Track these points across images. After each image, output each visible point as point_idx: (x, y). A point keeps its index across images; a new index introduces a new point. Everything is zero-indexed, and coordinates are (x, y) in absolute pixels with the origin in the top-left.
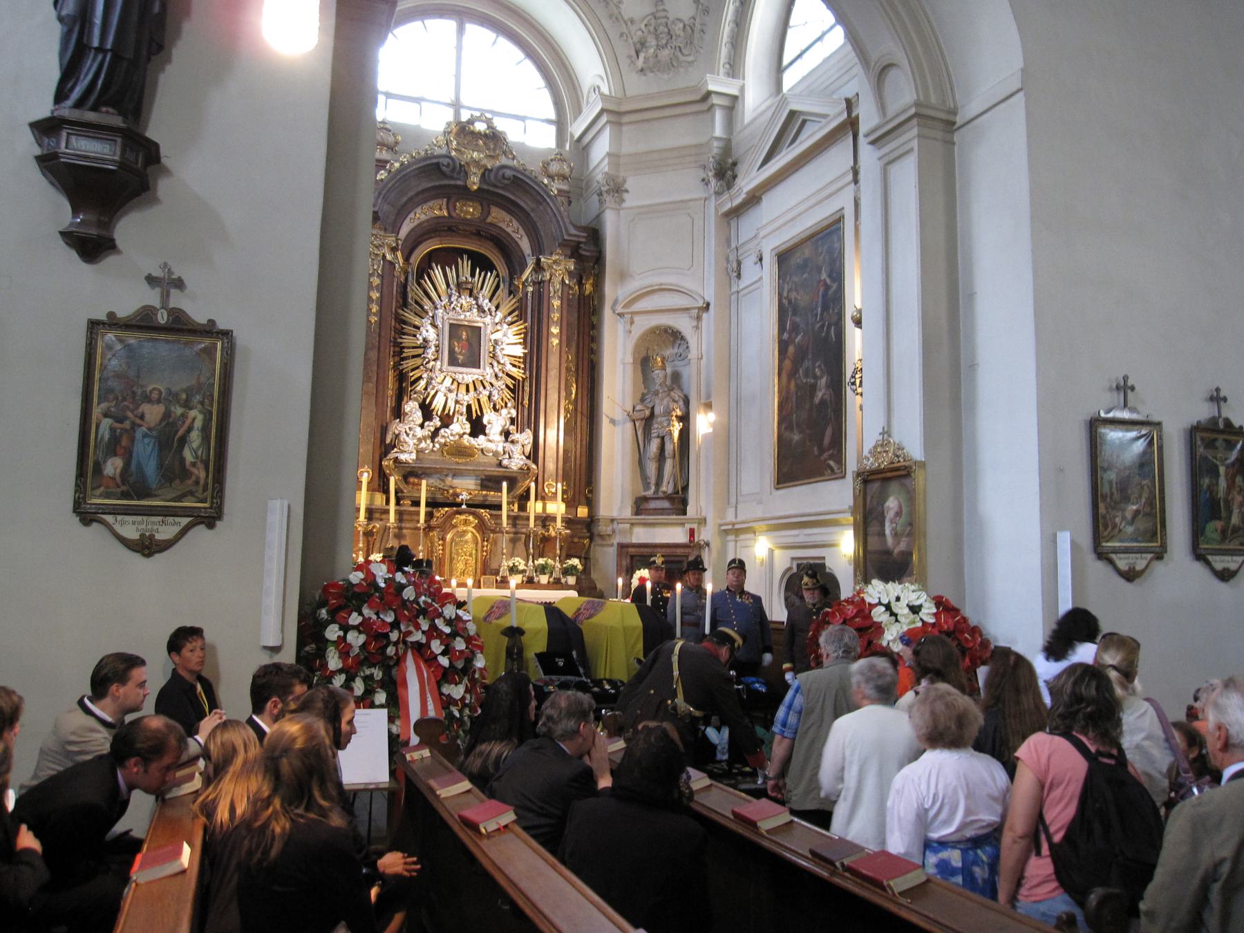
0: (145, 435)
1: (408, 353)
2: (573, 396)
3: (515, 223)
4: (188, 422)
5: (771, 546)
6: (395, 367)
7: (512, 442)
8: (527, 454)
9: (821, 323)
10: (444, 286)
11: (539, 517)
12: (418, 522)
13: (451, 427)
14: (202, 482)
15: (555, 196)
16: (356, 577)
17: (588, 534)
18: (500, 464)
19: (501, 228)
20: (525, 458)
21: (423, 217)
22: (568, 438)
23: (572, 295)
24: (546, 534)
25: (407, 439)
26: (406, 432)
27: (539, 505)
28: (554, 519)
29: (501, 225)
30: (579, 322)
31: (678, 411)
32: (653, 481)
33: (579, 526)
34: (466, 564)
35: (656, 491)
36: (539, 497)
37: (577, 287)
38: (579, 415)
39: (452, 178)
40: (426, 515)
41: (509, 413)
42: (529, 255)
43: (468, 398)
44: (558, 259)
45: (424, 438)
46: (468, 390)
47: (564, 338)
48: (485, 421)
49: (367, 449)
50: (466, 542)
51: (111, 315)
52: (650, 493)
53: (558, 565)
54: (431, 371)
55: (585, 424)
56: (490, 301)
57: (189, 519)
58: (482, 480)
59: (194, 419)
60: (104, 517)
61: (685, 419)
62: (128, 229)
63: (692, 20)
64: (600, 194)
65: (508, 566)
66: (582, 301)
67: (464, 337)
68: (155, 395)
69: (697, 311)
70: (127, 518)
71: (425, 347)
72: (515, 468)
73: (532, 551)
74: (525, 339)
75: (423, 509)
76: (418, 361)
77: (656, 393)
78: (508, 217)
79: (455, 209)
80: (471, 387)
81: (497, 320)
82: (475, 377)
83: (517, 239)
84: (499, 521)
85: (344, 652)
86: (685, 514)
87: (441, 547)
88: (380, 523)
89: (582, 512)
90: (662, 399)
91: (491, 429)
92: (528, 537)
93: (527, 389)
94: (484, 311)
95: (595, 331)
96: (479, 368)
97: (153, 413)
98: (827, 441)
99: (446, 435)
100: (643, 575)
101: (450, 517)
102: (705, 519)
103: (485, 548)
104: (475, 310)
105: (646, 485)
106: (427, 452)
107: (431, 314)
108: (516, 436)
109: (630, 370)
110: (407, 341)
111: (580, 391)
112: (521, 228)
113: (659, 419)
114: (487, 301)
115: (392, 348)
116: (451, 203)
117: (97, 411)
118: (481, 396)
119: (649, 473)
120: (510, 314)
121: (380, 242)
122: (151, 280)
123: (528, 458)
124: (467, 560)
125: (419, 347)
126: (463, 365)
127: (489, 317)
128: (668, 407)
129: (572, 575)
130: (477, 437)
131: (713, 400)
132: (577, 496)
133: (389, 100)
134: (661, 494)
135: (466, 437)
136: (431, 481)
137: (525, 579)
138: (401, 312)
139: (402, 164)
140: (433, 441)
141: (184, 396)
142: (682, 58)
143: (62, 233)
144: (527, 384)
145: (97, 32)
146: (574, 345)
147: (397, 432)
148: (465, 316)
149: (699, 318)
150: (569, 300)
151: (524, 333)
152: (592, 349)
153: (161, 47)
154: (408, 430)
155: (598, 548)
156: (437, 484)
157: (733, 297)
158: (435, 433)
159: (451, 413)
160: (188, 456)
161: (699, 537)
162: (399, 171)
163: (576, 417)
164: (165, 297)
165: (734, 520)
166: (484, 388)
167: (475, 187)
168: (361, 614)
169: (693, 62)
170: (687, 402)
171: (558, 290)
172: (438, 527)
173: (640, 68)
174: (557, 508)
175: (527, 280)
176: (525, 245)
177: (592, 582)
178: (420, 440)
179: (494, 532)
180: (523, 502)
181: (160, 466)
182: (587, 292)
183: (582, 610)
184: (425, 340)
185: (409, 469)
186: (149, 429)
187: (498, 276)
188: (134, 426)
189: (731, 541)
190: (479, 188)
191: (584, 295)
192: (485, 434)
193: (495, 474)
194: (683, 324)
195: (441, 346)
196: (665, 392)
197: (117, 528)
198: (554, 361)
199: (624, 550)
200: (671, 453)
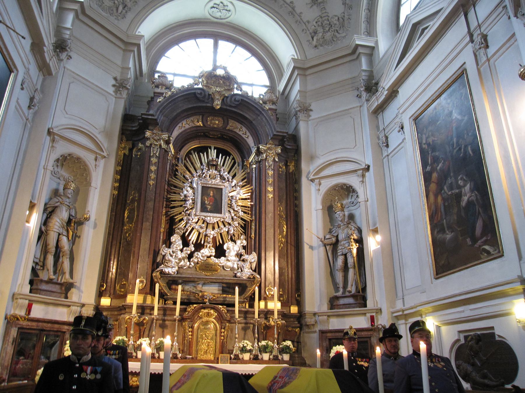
1: (174, 204)
2: (285, 233)
3: (244, 129)
5: (437, 323)
6: (166, 214)
7: (243, 261)
8: (253, 268)
9: (457, 149)
10: (199, 165)
11: (262, 311)
12: (175, 315)
13: (202, 251)
15: (267, 110)
17: (298, 325)
18: (235, 276)
19: (235, 132)
20: (251, 271)
21: (187, 126)
22: (282, 260)
23: (281, 171)
24: (268, 323)
25: (170, 258)
26: (170, 254)
27: (262, 304)
28: (271, 312)
29: (235, 130)
30: (286, 187)
31: (355, 235)
32: (341, 285)
33: (292, 319)
34: (208, 345)
35: (344, 292)
36: (262, 298)
37: (284, 167)
38: (289, 245)
39: (203, 102)
40: (180, 311)
41: (242, 243)
42: (253, 147)
43: (212, 233)
44: (271, 147)
45: (184, 259)
46: (213, 228)
47: (276, 193)
48: (225, 247)
50: (209, 329)
52: (340, 294)
53: (276, 345)
54: (189, 215)
55: (293, 251)
56: (229, 173)
58: (223, 287)
61: (360, 241)
63: (343, 14)
64: (296, 115)
65: (239, 347)
66: (288, 177)
67: (211, 194)
69: (362, 171)
71: (185, 201)
72: (245, 278)
73: (257, 336)
74: (251, 196)
75: (178, 306)
76: (180, 209)
77: (339, 226)
78: (239, 126)
79: (207, 122)
80: (216, 226)
81: (233, 184)
82: (219, 219)
83: (245, 138)
84: (233, 315)
86: (365, 306)
87: (190, 333)
88: (149, 316)
89: (294, 309)
90: (343, 230)
91: (229, 252)
92: (254, 326)
93: (253, 227)
94: (224, 179)
95: (297, 194)
96: (221, 213)
98: (478, 230)
99: (198, 256)
100: (339, 350)
101: (197, 311)
102: (381, 310)
104: (219, 178)
105: (337, 289)
106: (185, 268)
107: (190, 181)
108: (246, 257)
109: (320, 213)
110: (173, 197)
111: (289, 230)
112: (247, 131)
113: (342, 243)
114: (226, 173)
115: (165, 203)
116: (204, 118)
118: (222, 231)
119: (338, 281)
120: (242, 180)
121: (158, 138)
123: (255, 271)
124: (209, 343)
125: (181, 201)
126: (211, 212)
127: (228, 182)
128: (348, 234)
129: (287, 353)
130: (220, 258)
131: (378, 225)
132: (290, 299)
133: (175, 77)
134: (347, 294)
135: (212, 258)
136: (187, 287)
137: (252, 356)
138: (170, 179)
140: (189, 261)
142: (338, 35)
144: (253, 224)
146: (284, 202)
147: (163, 254)
148: (212, 182)
149: (363, 176)
150: (279, 174)
151: (251, 192)
152: (296, 204)
154: (171, 253)
155: (305, 335)
156: (191, 289)
157: (385, 160)
158: (190, 256)
159: (202, 242)
161: (377, 322)
162: (170, 97)
163: (287, 246)
165: (403, 308)
166: (225, 226)
167: (218, 107)
169: (345, 36)
170: (360, 231)
171: (271, 165)
172: (189, 319)
173: (315, 45)
174: (275, 305)
175: (252, 161)
176: (250, 141)
177: (303, 359)
178: (180, 260)
179: (229, 322)
180: (251, 302)
182: (291, 171)
183: (277, 379)
184: (186, 196)
185: (171, 279)
187: (233, 159)
189: (402, 324)
190: (220, 108)
191: (289, 173)
192: (225, 256)
193: (230, 281)
194: (353, 181)
195: (196, 200)
196: (345, 225)
198: (270, 208)
199: (324, 335)
200: (352, 264)
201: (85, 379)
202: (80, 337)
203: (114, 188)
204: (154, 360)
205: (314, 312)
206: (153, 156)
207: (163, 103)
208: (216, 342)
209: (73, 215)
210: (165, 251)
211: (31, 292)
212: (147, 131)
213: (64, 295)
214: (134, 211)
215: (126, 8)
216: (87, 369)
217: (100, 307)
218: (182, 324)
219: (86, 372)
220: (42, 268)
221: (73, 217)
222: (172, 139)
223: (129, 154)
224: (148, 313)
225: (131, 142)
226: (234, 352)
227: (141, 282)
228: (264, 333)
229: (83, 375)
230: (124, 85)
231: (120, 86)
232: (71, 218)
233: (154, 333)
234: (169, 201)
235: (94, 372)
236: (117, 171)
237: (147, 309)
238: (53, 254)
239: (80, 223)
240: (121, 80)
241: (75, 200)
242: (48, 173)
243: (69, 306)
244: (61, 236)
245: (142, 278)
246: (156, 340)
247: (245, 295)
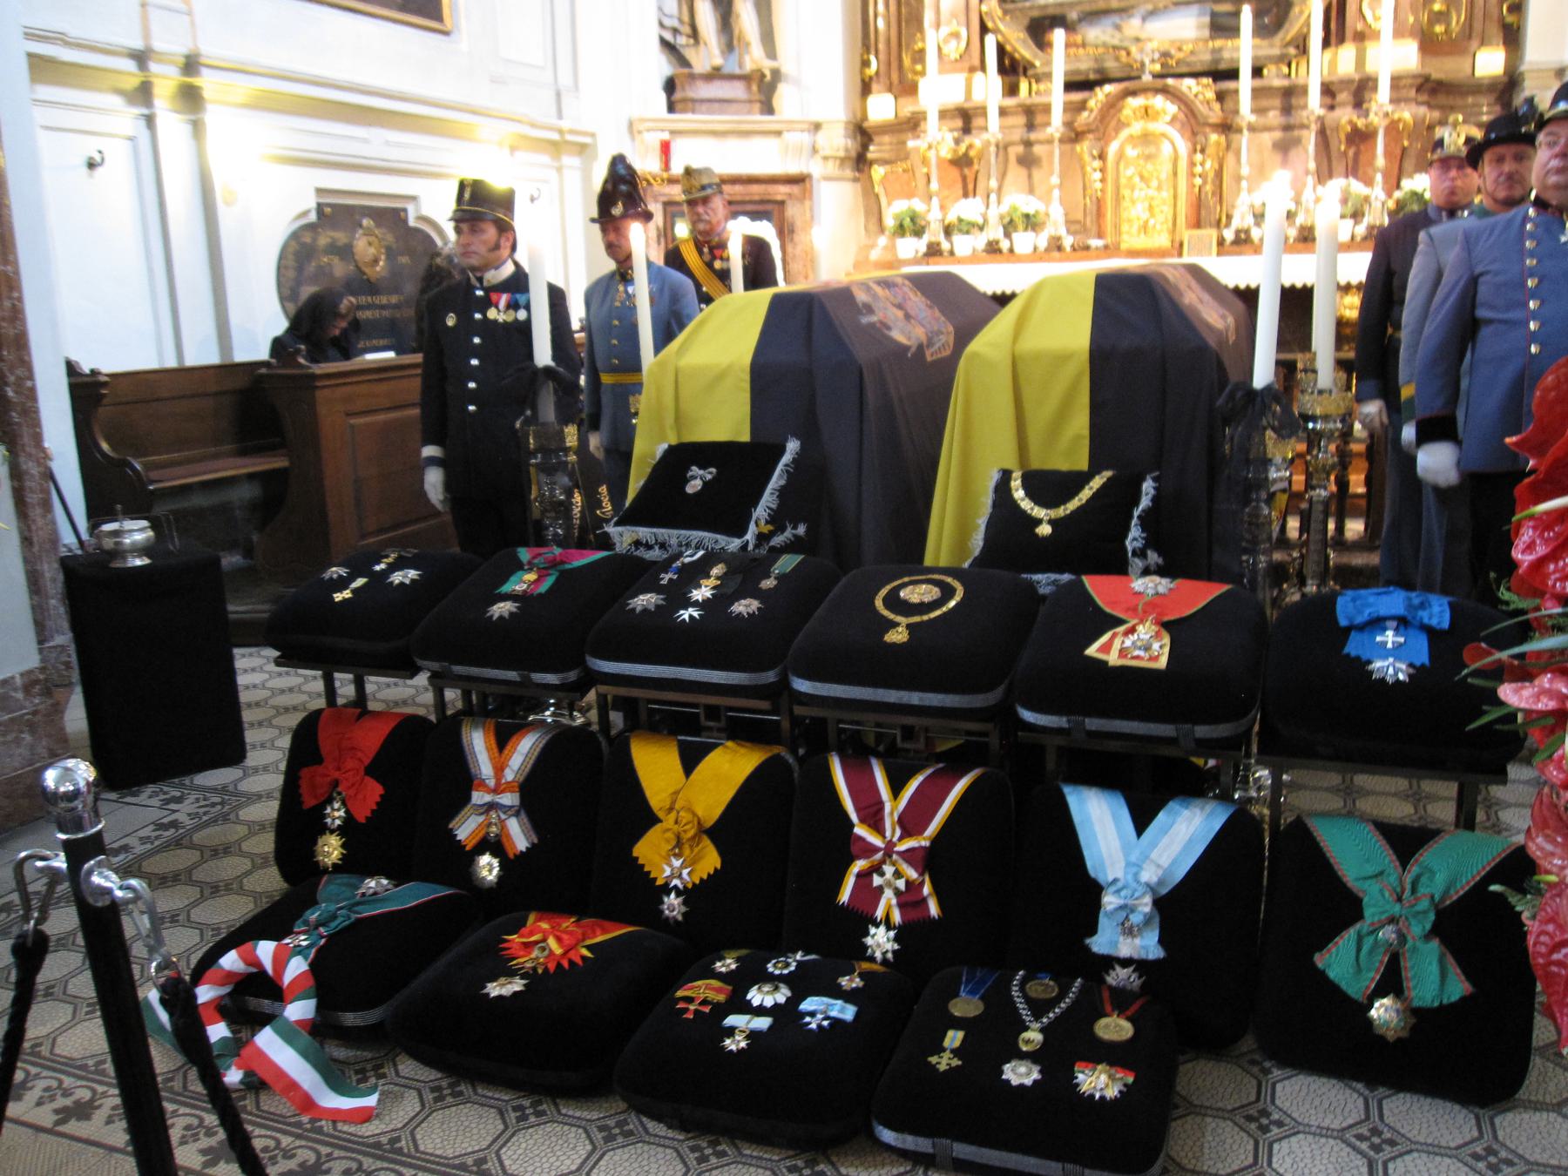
36: (1349, 33)
53: (1377, 192)
58: (1214, 15)
101: (1113, 105)
103: (1198, 169)
124: (1152, 199)
132: (1478, 25)
172: (1089, 131)
201: (495, 321)
204: (998, 257)
205: (1557, 66)
208: (1175, 197)
211: (671, 108)
216: (499, 298)
217: (866, 125)
218: (1073, 150)
219: (497, 307)
226: (1236, 223)
228: (1351, 153)
229: (492, 314)
237: (976, 115)
245: (954, 27)
247: (1287, 32)
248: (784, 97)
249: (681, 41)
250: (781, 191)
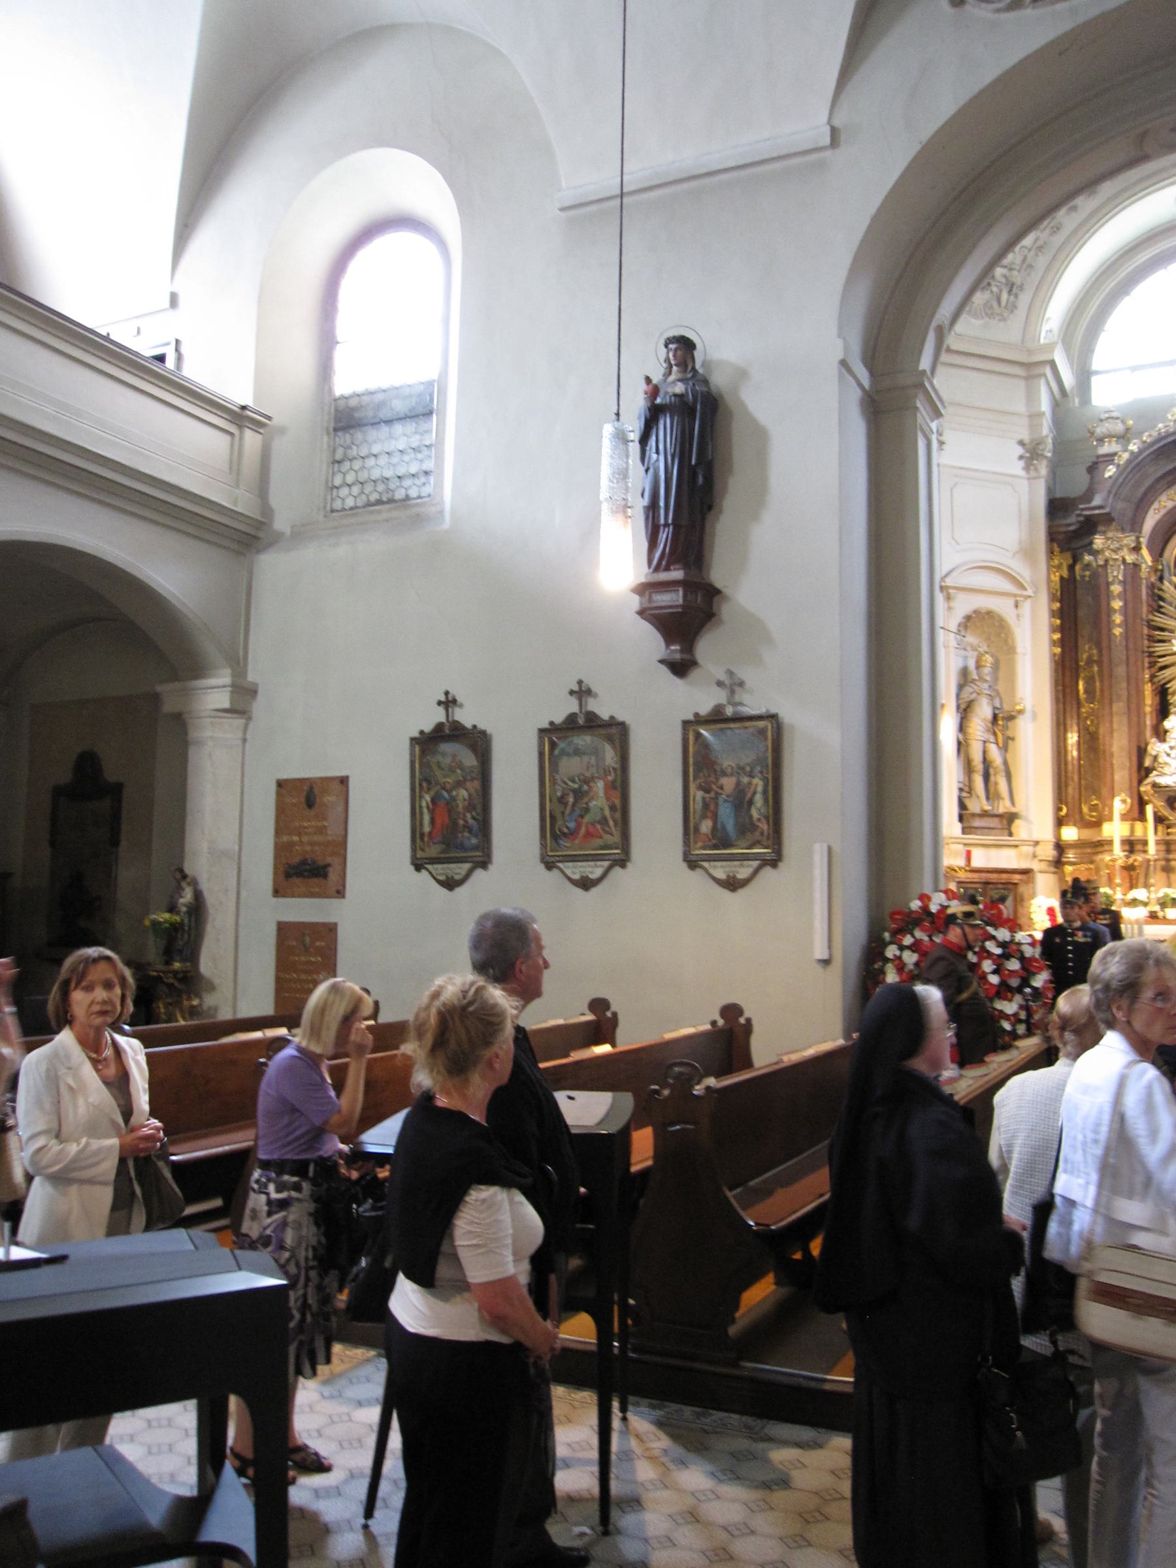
0: (726, 801)
4: (753, 787)
6: (1151, 680)
14: (766, 834)
16: (916, 905)
25: (1167, 759)
49: (1121, 773)
51: (696, 715)
57: (758, 862)
59: (756, 785)
60: (703, 863)
62: (704, 648)
68: (729, 771)
70: (716, 863)
85: (900, 966)
88: (1143, 855)
97: (728, 783)
110: (1160, 649)
115: (1147, 660)
117: (692, 787)
122: (720, 684)
138: (1151, 617)
139: (1132, 453)
141: (748, 769)
143: (662, 662)
145: (662, 512)
147: (1154, 753)
153: (710, 508)
160: (755, 814)
162: (1129, 462)
164: (733, 692)
168: (913, 936)
181: (737, 824)
186: (728, 796)
188: (717, 794)
197: (712, 871)
202: (1068, 906)
203: (1054, 643)
206: (1113, 583)
207: (1117, 479)
209: (999, 706)
210: (1155, 747)
212: (1094, 538)
213: (1006, 832)
214: (1094, 682)
215: (1015, 290)
217: (1061, 843)
220: (969, 795)
221: (999, 709)
222: (1144, 541)
223: (1069, 575)
224: (1140, 851)
225: (1068, 555)
227: (1124, 801)
229: (1076, 938)
230: (1040, 452)
231: (1031, 454)
232: (997, 712)
233: (1152, 881)
234: (1151, 654)
235: (1085, 936)
236: (1053, 610)
237: (1137, 844)
238: (981, 773)
239: (1011, 718)
240: (1032, 441)
241: (996, 679)
242: (952, 650)
243: (1016, 846)
244: (987, 745)
246: (1156, 891)
248: (1019, 827)
249: (964, 794)
250: (1016, 878)
